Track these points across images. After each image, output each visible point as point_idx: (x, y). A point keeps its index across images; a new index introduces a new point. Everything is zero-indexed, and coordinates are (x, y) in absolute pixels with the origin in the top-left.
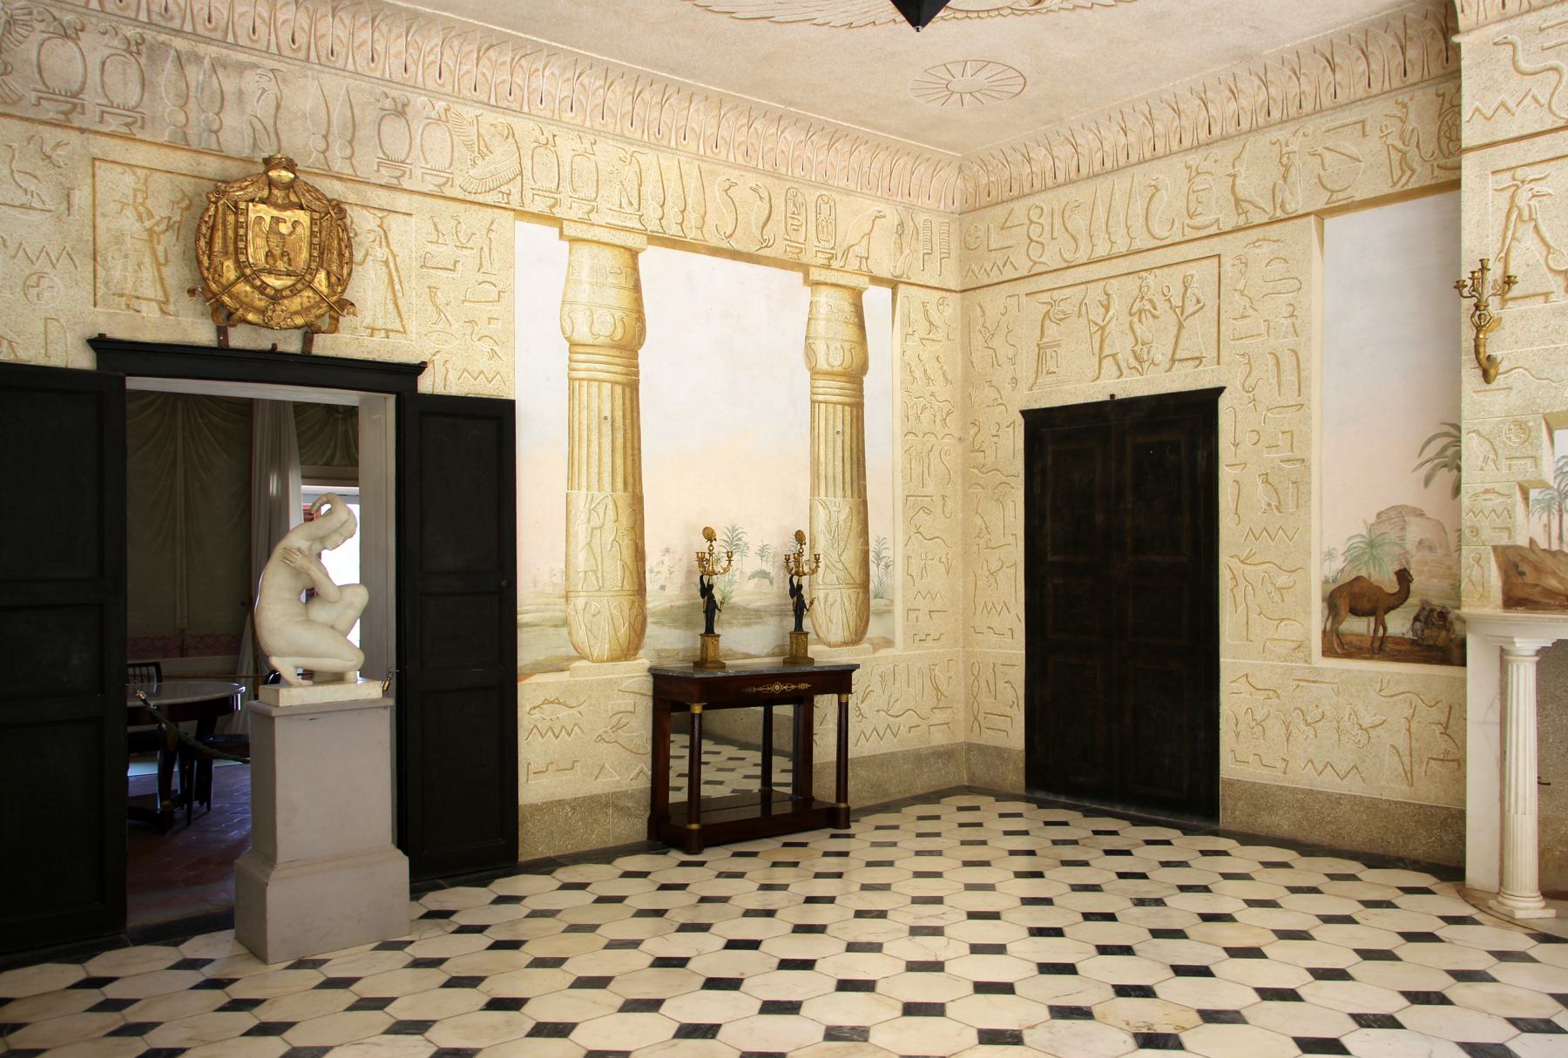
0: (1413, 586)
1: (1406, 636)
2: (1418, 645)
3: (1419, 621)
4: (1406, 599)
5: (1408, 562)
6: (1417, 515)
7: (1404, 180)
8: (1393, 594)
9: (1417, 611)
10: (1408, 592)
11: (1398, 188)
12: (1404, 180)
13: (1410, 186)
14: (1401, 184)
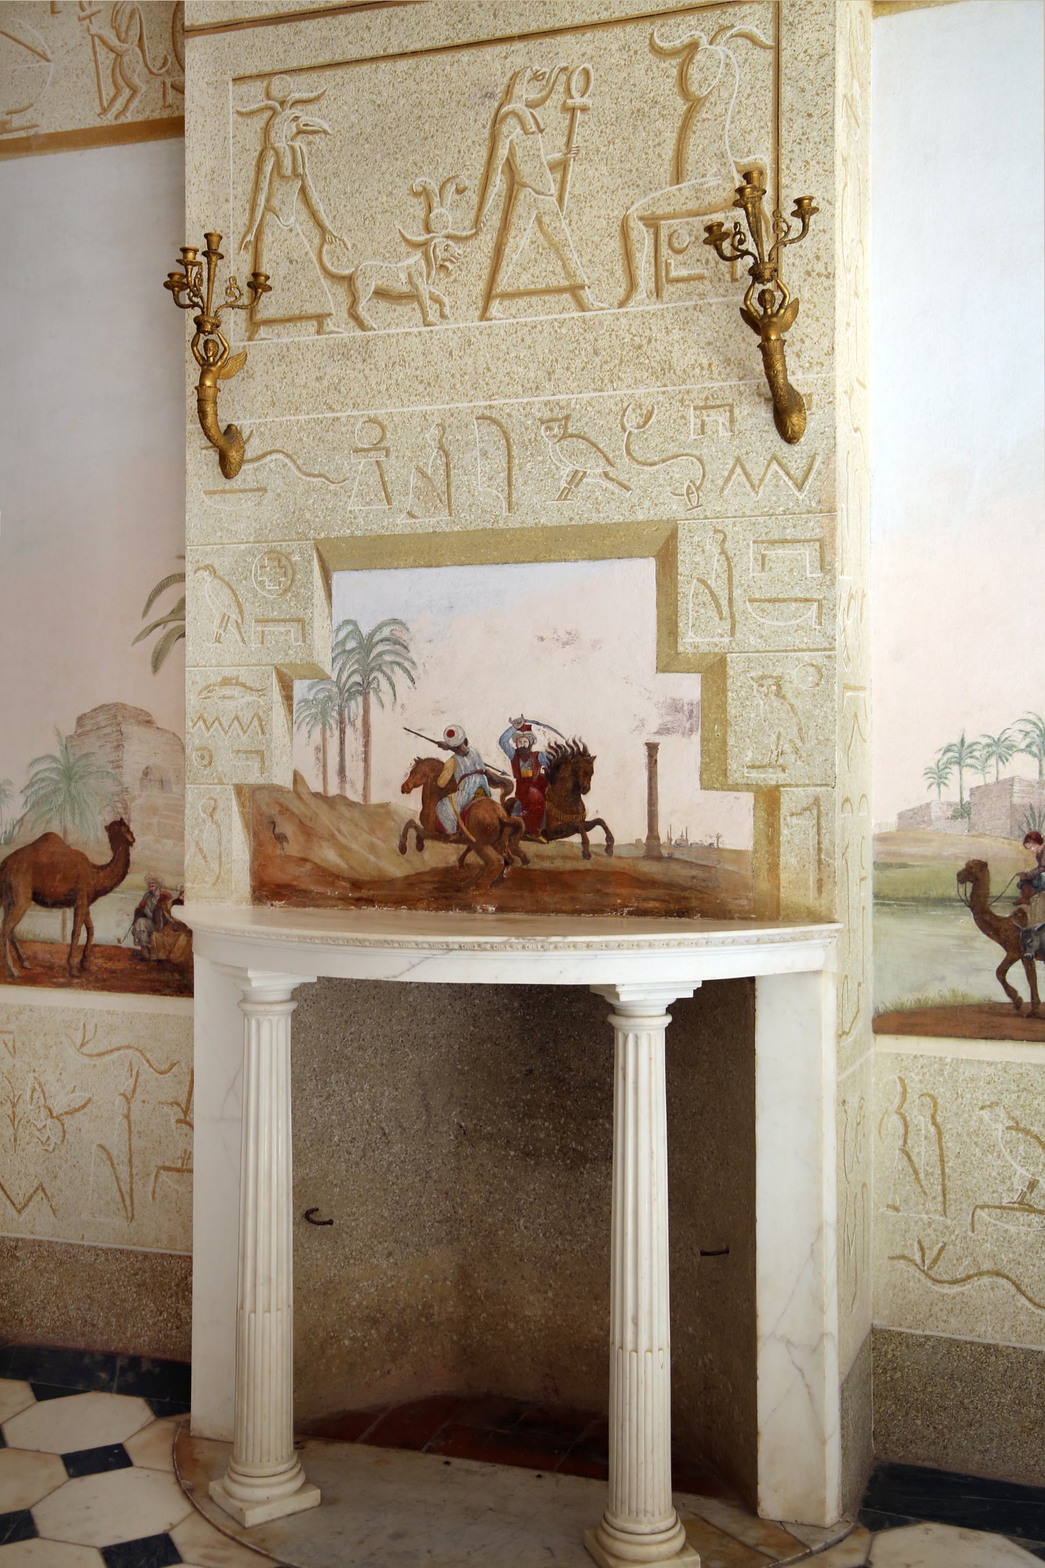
0: (134, 853)
1: (124, 945)
2: (143, 959)
3: (145, 916)
4: (123, 877)
5: (126, 808)
6: (140, 723)
7: (119, 105)
8: (102, 868)
9: (140, 899)
10: (127, 863)
11: (109, 120)
12: (119, 105)
13: (129, 118)
14: (114, 111)
